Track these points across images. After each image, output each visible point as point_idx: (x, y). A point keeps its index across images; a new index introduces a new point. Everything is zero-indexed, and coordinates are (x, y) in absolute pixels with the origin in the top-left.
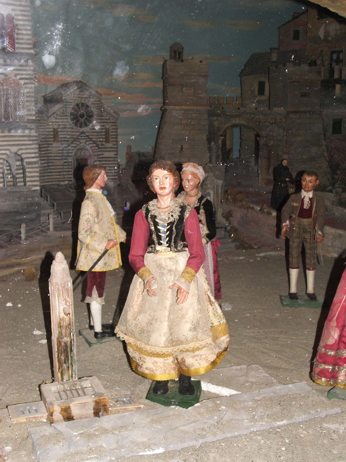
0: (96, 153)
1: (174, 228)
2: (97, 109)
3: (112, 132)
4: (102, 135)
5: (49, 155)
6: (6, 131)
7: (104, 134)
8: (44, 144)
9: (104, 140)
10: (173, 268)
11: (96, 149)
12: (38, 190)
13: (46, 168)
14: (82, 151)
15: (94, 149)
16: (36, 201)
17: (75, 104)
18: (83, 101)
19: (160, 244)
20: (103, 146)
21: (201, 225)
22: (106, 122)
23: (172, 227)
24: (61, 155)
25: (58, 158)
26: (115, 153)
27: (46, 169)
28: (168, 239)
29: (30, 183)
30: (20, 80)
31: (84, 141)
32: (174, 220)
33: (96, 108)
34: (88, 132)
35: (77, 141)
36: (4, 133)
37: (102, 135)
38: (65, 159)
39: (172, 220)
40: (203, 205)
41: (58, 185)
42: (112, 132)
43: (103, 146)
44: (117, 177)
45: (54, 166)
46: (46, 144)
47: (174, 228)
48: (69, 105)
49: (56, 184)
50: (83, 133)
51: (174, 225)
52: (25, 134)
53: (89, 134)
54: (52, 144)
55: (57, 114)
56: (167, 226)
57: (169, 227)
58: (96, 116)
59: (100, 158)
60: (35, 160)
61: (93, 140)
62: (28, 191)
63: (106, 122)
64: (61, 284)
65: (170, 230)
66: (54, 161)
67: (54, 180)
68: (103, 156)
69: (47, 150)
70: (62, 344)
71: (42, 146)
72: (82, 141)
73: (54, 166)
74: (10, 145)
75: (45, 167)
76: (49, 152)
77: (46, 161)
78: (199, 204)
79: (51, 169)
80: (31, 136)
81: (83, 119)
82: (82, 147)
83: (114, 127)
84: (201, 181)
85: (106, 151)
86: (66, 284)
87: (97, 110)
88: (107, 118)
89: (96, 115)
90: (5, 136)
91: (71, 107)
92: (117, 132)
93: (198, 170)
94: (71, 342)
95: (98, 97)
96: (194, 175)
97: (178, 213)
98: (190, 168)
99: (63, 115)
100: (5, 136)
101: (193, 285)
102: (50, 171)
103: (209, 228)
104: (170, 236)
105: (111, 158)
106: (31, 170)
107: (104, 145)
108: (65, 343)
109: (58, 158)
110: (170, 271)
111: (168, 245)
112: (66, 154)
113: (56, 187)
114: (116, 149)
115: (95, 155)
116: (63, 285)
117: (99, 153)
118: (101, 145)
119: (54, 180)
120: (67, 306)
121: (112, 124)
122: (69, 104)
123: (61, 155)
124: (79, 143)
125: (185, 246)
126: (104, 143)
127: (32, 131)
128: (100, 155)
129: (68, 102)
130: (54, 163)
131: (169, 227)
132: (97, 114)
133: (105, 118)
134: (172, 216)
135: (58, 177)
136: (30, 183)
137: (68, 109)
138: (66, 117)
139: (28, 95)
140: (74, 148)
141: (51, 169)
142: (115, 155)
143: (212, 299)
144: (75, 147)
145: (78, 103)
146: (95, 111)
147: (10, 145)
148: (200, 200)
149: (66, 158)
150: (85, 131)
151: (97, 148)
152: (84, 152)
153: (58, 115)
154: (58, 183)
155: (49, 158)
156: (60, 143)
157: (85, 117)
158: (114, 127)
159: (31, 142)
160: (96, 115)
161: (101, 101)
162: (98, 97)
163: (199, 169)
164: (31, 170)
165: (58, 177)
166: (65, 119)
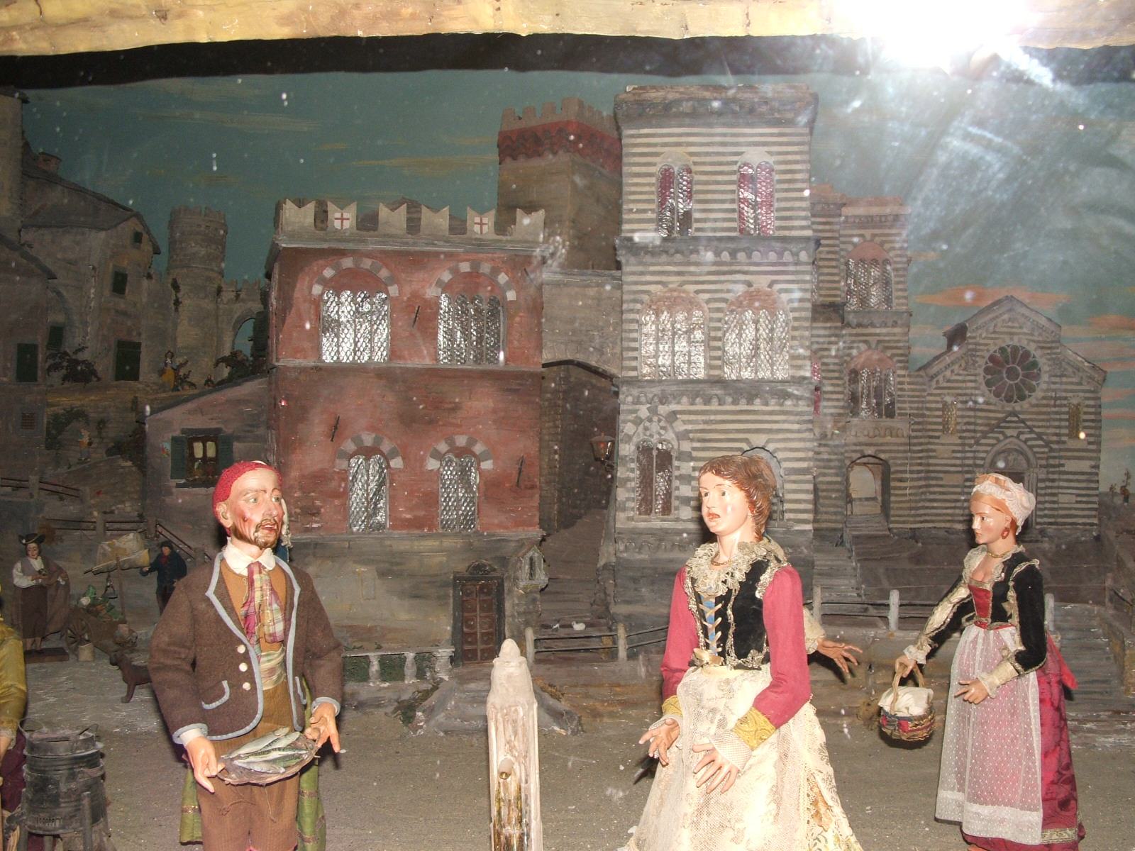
0: (1044, 462)
1: (729, 612)
2: (1049, 360)
3: (1086, 413)
4: (1060, 420)
5: (931, 461)
6: (744, 401)
7: (1067, 417)
8: (921, 437)
9: (1066, 431)
10: (720, 705)
11: (1043, 453)
12: (810, 530)
13: (921, 490)
14: (1009, 455)
15: (1038, 453)
16: (802, 556)
17: (997, 348)
18: (1015, 342)
19: (707, 646)
20: (1062, 446)
21: (806, 612)
22: (1072, 391)
23: (725, 607)
24: (958, 462)
25: (952, 469)
26: (1093, 463)
27: (922, 493)
28: (719, 634)
29: (792, 516)
30: (780, 293)
31: (1014, 433)
32: (730, 591)
33: (1049, 357)
34: (1023, 413)
35: (997, 432)
36: (738, 404)
37: (1060, 420)
38: (968, 472)
39: (722, 591)
40: (1020, 580)
41: (948, 530)
42: (1086, 413)
43: (1062, 446)
44: (1096, 521)
45: (941, 486)
46: (925, 437)
47: (729, 612)
48: (982, 350)
49: (945, 528)
50: (1014, 414)
51: (730, 605)
52: (784, 408)
53: (1028, 417)
54: (938, 437)
55: (952, 371)
56: (716, 604)
57: (720, 606)
58: (1047, 375)
59: (1053, 473)
60: (804, 465)
61: (1037, 430)
62: (785, 533)
63: (1072, 391)
64: (502, 709)
65: (721, 613)
66: (941, 475)
67: (941, 518)
68: (1062, 469)
69: (927, 451)
70: (502, 838)
71: (915, 441)
72: (1009, 432)
73: (941, 486)
74: (749, 431)
75: (920, 487)
76: (931, 454)
77: (923, 475)
78: (1003, 575)
79: (934, 493)
80: (798, 414)
81: (1012, 382)
82: (1009, 446)
83: (1092, 403)
84: (1020, 523)
85: (1069, 458)
86: (513, 709)
87: (1050, 363)
88: (1074, 380)
89: (1046, 372)
90: (741, 412)
91: (987, 355)
92: (1100, 413)
93: (1008, 493)
94: (521, 839)
95: (1052, 332)
96: (1000, 507)
97: (740, 576)
98: (987, 486)
99: (966, 373)
100: (741, 412)
101: (767, 753)
102: (932, 497)
103: (1025, 638)
104: (723, 627)
105: (1083, 473)
106: (794, 486)
107: (1064, 442)
108: (506, 838)
109: (952, 469)
110: (713, 711)
111: (720, 649)
112: (971, 462)
113: (942, 533)
114: (1095, 455)
115: (1041, 466)
116: (505, 711)
117: (1052, 462)
118: (1058, 442)
119: (941, 518)
120: (512, 759)
121: (1088, 395)
122: (981, 347)
123: (958, 462)
124: (1001, 437)
125: (766, 659)
126: (1064, 438)
127: (800, 402)
128: (1054, 466)
129: (980, 344)
130: (941, 479)
131: (720, 606)
132: (1050, 371)
133: (1070, 380)
134: (725, 582)
135: (949, 511)
136: (792, 516)
137: (978, 359)
138: (973, 378)
139: (796, 324)
140: (989, 448)
141: (934, 493)
142: (1093, 467)
143: (830, 796)
144: (993, 445)
145: (1004, 345)
146: (1045, 364)
147: (749, 431)
148: (1009, 565)
149: (971, 468)
150: (1018, 408)
151: (1046, 450)
152: (1015, 460)
153: (956, 372)
154: (948, 525)
155: (931, 468)
156: (959, 435)
157: (1021, 377)
158: (1092, 403)
159: (796, 427)
160: (1046, 372)
161: (1059, 342)
162: (1052, 332)
163: (1008, 490)
164: (794, 486)
165: (949, 511)
166: (971, 381)
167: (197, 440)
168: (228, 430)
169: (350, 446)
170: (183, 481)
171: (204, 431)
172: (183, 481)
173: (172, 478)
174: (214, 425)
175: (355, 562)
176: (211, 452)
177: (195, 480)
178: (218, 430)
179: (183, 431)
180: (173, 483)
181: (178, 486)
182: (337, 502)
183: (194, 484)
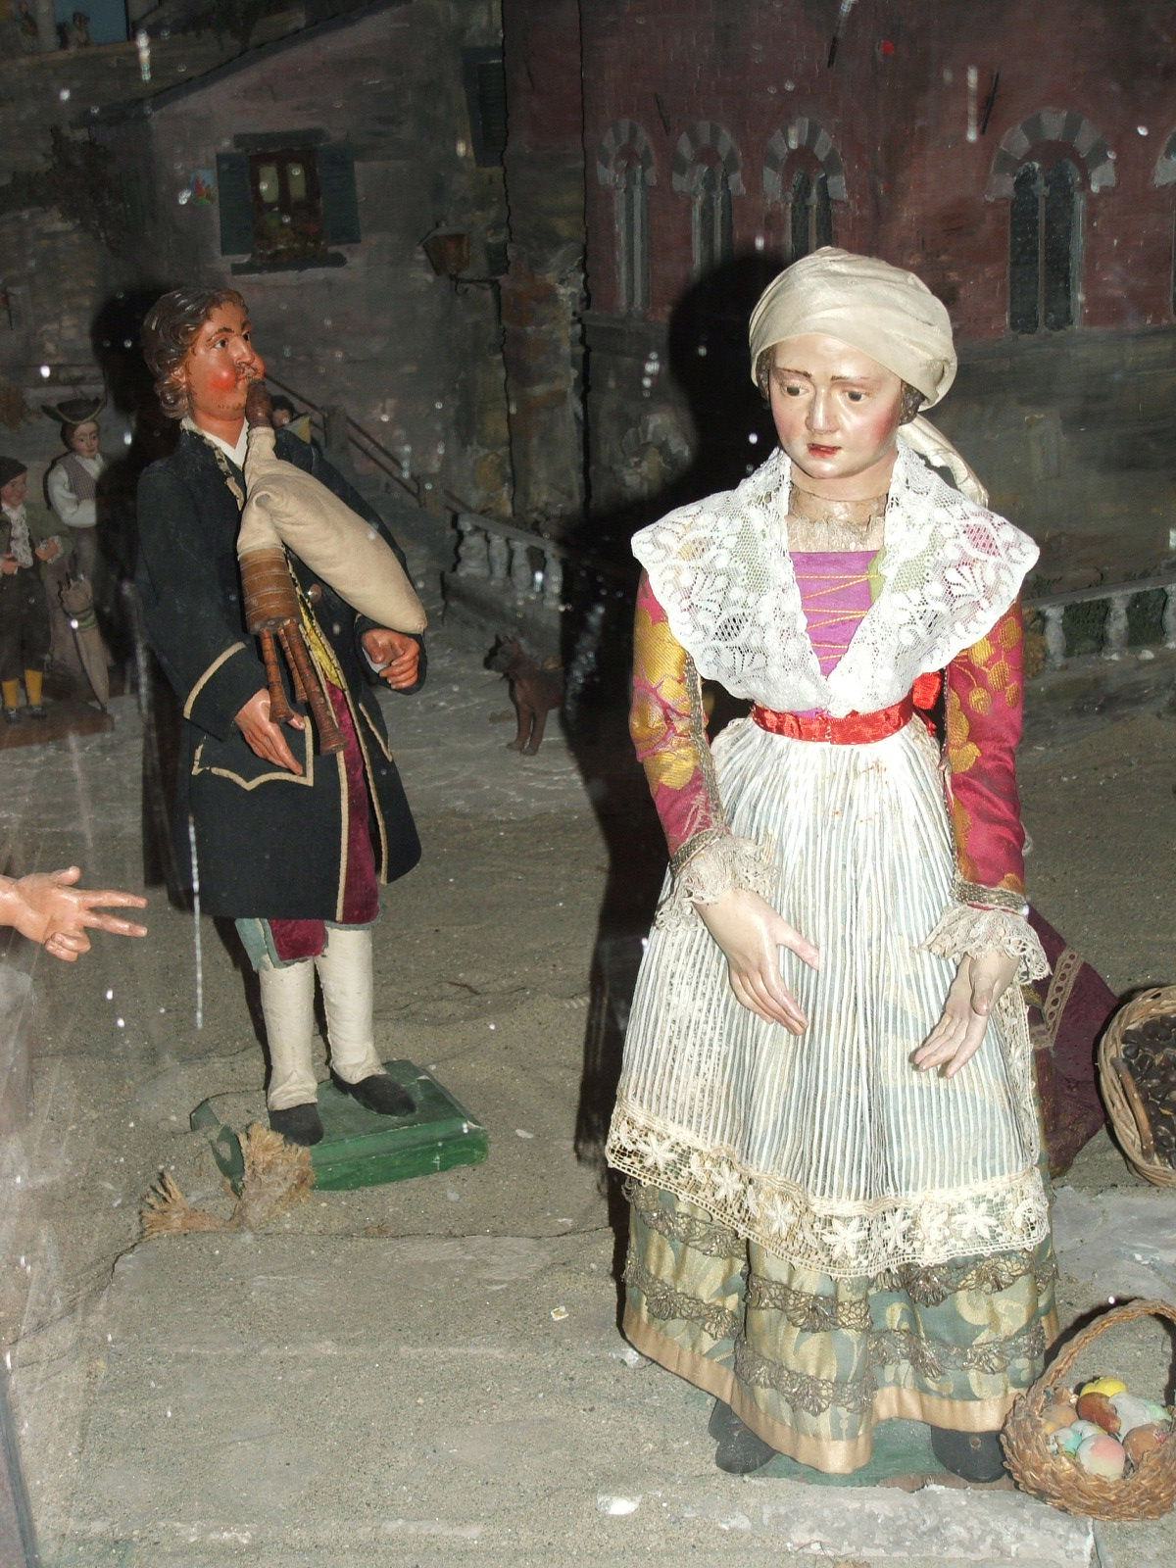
167: (266, 159)
168: (335, 132)
169: (1018, 141)
170: (245, 259)
171: (286, 137)
172: (245, 259)
173: (224, 252)
174: (300, 124)
175: (1023, 402)
176: (298, 190)
177: (278, 253)
178: (316, 134)
179: (239, 140)
180: (223, 263)
181: (238, 269)
182: (989, 272)
183: (275, 263)
